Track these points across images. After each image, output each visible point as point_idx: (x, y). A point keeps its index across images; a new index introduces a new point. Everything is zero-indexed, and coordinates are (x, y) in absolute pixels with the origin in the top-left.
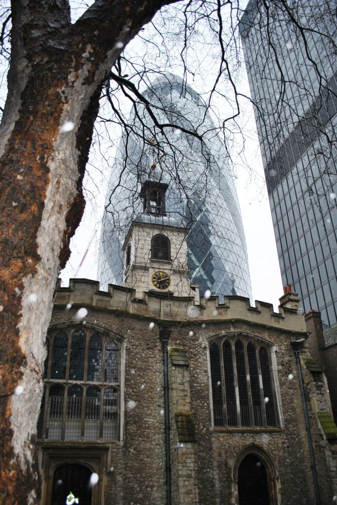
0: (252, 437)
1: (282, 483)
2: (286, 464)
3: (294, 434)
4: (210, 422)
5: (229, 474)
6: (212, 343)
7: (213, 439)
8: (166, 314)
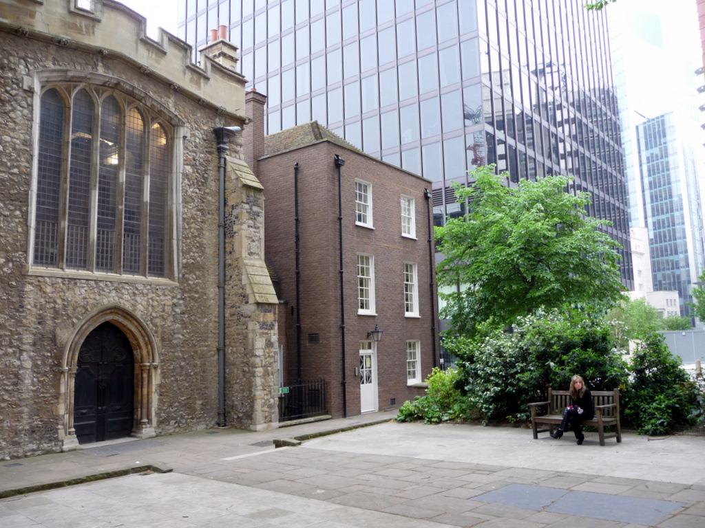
0: (116, 289)
1: (164, 376)
2: (175, 342)
3: (196, 292)
4: (26, 252)
5: (58, 358)
6: (49, 86)
7: (28, 288)
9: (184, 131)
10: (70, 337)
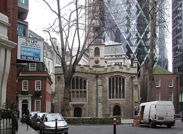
8: (98, 72)
9: (126, 78)
10: (112, 107)
